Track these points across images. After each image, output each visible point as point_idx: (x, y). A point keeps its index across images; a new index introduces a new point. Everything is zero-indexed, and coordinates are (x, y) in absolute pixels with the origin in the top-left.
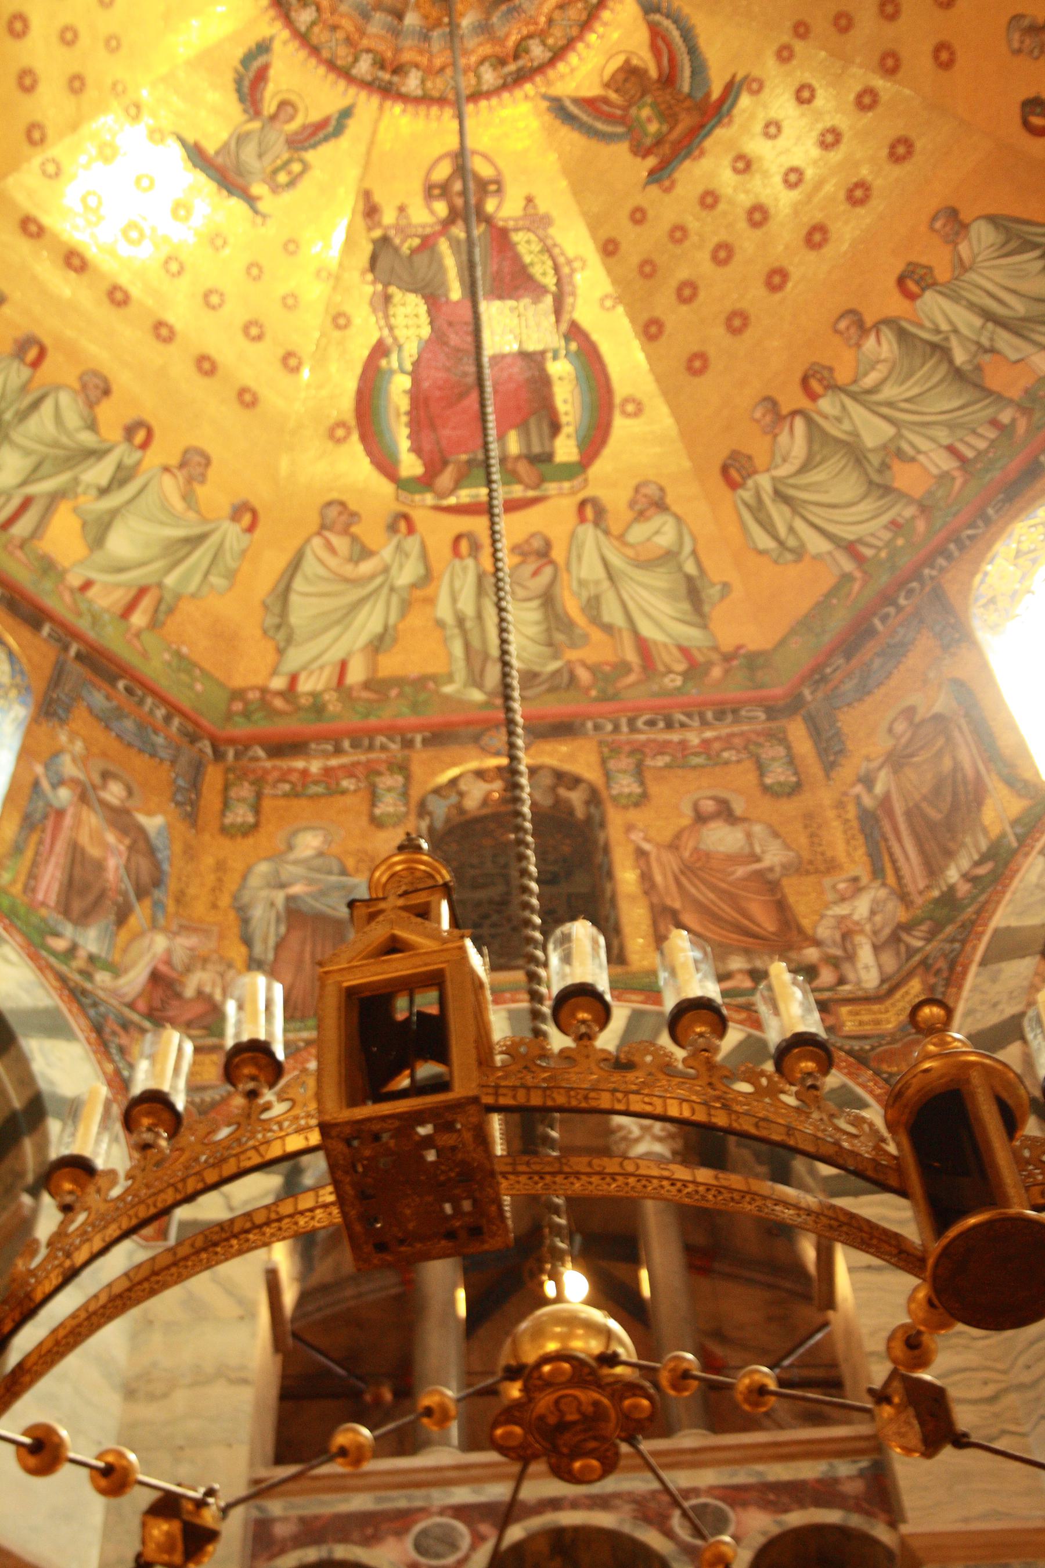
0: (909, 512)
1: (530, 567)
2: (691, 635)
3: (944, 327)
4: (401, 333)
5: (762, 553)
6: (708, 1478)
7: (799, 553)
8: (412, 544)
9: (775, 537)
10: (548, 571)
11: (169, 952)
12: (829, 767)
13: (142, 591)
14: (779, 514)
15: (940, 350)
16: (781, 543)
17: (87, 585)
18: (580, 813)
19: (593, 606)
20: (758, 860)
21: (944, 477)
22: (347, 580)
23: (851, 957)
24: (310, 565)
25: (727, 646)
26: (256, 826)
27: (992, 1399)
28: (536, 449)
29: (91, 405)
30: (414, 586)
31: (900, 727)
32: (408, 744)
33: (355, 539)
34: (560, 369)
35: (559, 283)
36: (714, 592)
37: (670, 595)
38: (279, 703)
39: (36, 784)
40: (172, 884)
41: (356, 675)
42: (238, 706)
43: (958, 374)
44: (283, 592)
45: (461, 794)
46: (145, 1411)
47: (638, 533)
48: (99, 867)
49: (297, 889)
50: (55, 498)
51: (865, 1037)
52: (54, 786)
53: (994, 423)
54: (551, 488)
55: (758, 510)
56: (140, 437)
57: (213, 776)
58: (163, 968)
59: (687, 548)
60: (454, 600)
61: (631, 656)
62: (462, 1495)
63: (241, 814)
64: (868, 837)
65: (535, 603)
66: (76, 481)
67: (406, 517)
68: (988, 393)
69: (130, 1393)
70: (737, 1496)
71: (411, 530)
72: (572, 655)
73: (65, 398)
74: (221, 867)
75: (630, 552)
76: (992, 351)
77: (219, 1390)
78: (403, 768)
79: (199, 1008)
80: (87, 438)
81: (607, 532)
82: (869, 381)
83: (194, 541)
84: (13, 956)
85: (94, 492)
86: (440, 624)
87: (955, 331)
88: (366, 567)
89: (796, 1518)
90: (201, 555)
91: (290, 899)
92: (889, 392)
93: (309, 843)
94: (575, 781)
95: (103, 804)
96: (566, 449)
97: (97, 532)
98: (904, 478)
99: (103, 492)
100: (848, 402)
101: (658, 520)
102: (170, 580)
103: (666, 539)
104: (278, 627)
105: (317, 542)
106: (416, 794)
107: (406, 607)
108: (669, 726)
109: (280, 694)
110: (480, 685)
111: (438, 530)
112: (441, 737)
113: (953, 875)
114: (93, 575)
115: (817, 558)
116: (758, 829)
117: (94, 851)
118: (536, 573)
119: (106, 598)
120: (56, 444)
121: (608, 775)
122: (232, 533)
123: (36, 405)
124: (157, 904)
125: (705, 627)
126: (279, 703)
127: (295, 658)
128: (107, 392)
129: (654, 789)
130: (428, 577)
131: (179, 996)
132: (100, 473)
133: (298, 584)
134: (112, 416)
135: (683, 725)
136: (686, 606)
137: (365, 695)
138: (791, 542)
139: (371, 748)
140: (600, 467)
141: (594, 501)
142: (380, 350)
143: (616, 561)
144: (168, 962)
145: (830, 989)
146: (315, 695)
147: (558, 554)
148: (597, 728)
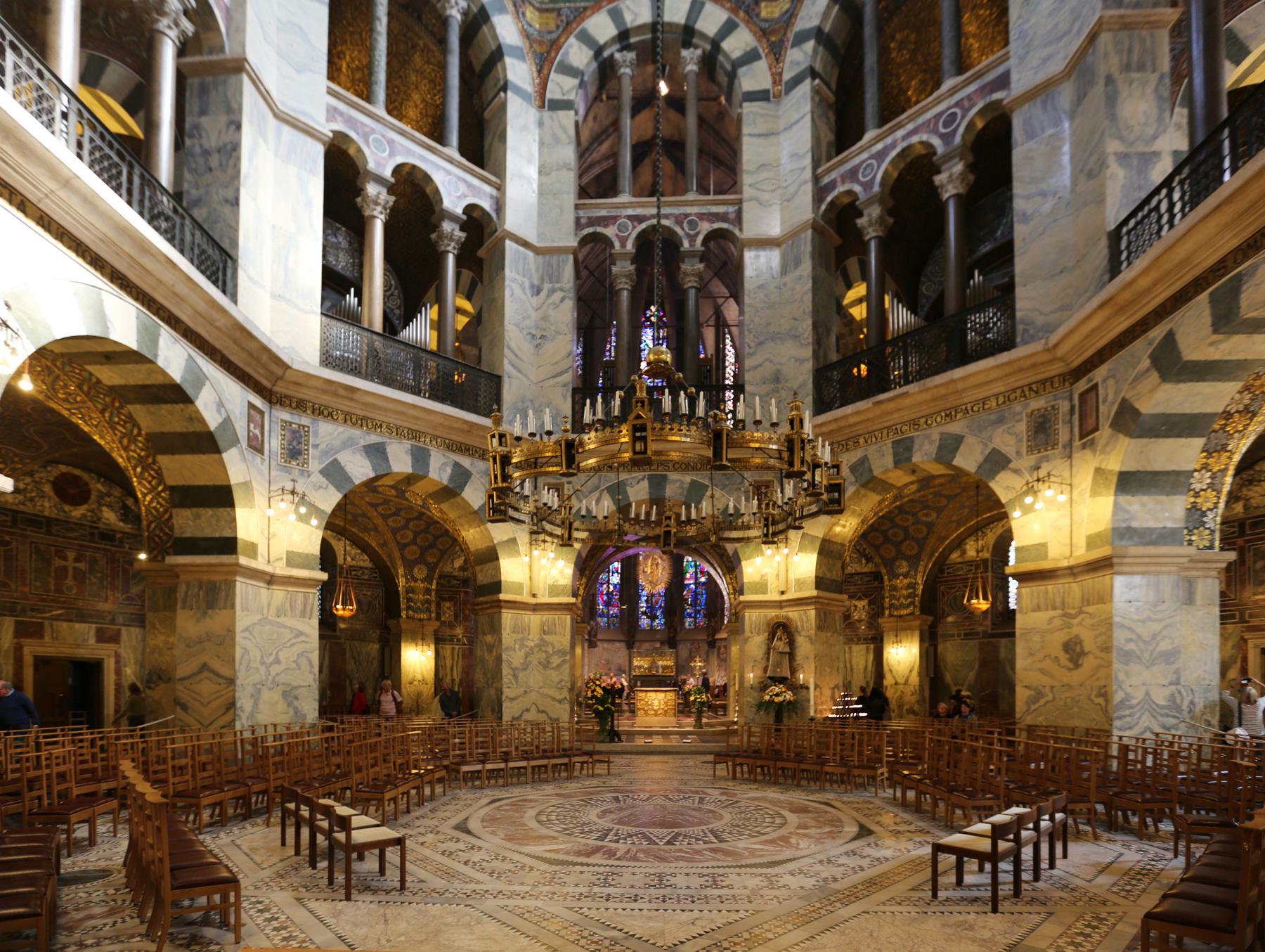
27: (773, 191)
51: (766, 20)
69: (540, 173)
70: (701, 216)
77: (564, 172)
89: (716, 225)
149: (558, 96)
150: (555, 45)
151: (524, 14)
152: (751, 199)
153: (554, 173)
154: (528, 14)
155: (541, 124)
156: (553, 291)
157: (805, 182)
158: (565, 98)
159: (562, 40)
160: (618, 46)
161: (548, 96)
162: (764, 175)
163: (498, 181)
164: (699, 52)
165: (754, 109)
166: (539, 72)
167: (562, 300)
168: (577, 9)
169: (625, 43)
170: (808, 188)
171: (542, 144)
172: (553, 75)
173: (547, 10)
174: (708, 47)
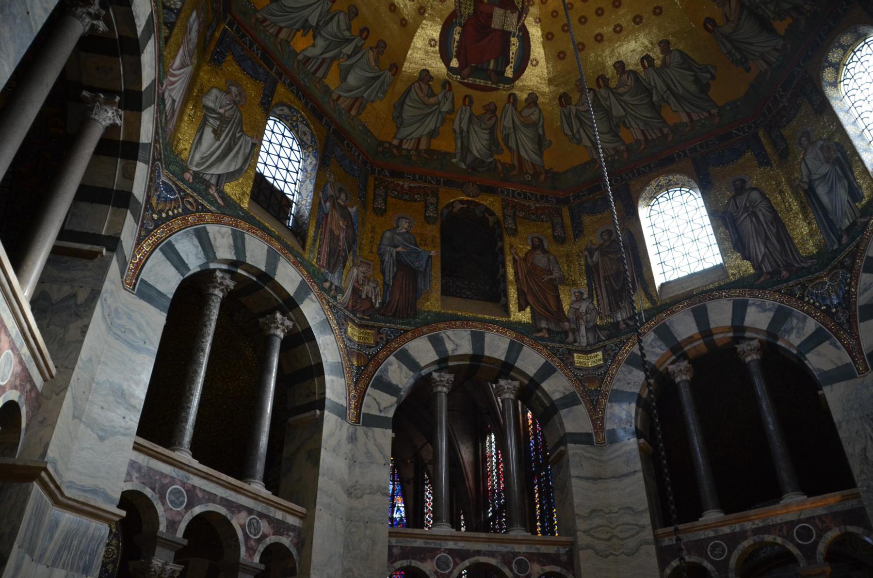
0: (622, 148)
1: (488, 116)
2: (536, 157)
3: (652, 84)
4: (463, 10)
5: (567, 135)
6: (523, 549)
7: (579, 142)
8: (449, 95)
9: (572, 131)
10: (494, 119)
11: (357, 275)
12: (576, 236)
13: (356, 99)
14: (575, 124)
15: (648, 92)
16: (574, 135)
17: (339, 97)
18: (491, 224)
19: (506, 138)
20: (552, 274)
21: (638, 141)
22: (424, 104)
23: (578, 330)
24: (413, 94)
25: (547, 168)
26: (385, 211)
28: (499, 69)
29: (350, 20)
30: (447, 112)
31: (606, 237)
32: (438, 182)
33: (430, 87)
34: (514, 40)
35: (522, 8)
38: (395, 151)
39: (320, 203)
40: (358, 242)
41: (423, 146)
42: (380, 149)
43: (652, 104)
44: (401, 103)
45: (453, 207)
46: (356, 503)
47: (526, 113)
48: (339, 240)
49: (399, 249)
50: (333, 59)
51: (579, 369)
52: (325, 203)
53: (661, 131)
54: (501, 86)
55: (568, 118)
56: (365, 34)
57: (371, 181)
58: (356, 285)
59: (541, 124)
60: (460, 123)
61: (516, 163)
62: (451, 545)
63: (380, 204)
64: (588, 278)
65: (487, 132)
66: (341, 52)
67: (449, 83)
68: (662, 118)
71: (450, 89)
72: (497, 157)
73: (342, 16)
74: (373, 230)
76: (667, 102)
77: (379, 497)
78: (436, 195)
80: (347, 33)
81: (516, 109)
82: (621, 90)
83: (375, 78)
84: (314, 298)
85: (346, 57)
86: (454, 131)
87: (656, 88)
88: (432, 100)
90: (377, 84)
91: (397, 253)
92: (626, 98)
93: (404, 225)
94: (492, 214)
95: (339, 204)
96: (509, 73)
97: (344, 74)
98: (623, 133)
99: (349, 57)
100: (611, 94)
101: (533, 109)
102: (365, 95)
103: (534, 117)
104: (398, 117)
105: (416, 84)
106: (440, 208)
107: (444, 121)
108: (525, 198)
109: (395, 146)
110: (465, 163)
111: (460, 91)
112: (449, 183)
113: (620, 317)
114: (341, 93)
115: (586, 147)
116: (551, 257)
117: (336, 232)
118: (489, 119)
119: (344, 104)
120: (336, 36)
121: (505, 219)
122: (388, 74)
123: (331, 19)
124: (355, 252)
125: (541, 156)
126: (395, 151)
127: (404, 132)
128: (357, 15)
129: (519, 228)
130: (452, 111)
131: (360, 296)
132: (348, 49)
133: (408, 101)
134: (356, 24)
135: (530, 199)
137: (425, 155)
138: (577, 136)
139: (425, 181)
140: (519, 83)
141: (514, 95)
142: (453, 15)
144: (357, 282)
146: (408, 151)
147: (498, 114)
148: (502, 192)
149: (374, 412)
153: (366, 497)
154: (349, 330)
155: (353, 439)
157: (647, 543)
158: (382, 414)
159: (381, 356)
160: (436, 367)
162: (598, 521)
163: (303, 510)
164: (516, 384)
165: (579, 451)
166: (356, 383)
169: (443, 365)
170: (652, 549)
171: (353, 461)
172: (370, 390)
173: (366, 327)
174: (526, 382)
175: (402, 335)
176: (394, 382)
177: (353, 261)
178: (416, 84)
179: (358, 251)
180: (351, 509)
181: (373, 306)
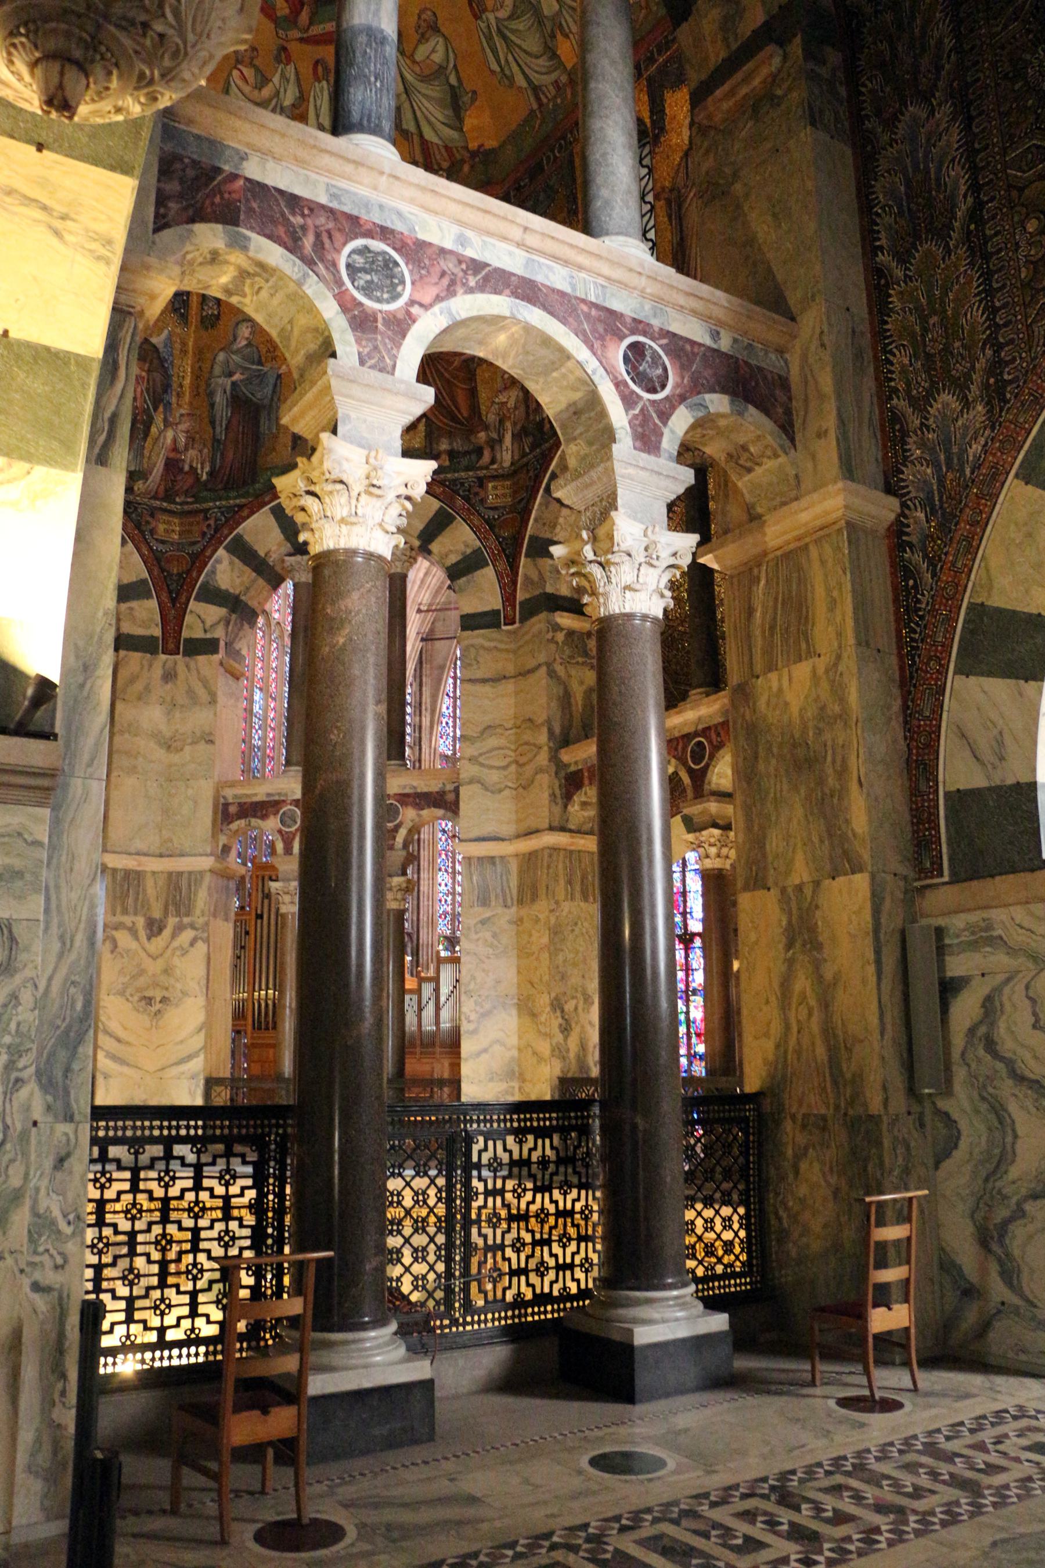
5: (493, 72)
7: (511, 79)
8: (290, 70)
11: (175, 440)
23: (501, 441)
25: (473, 145)
36: (466, 99)
37: (440, 103)
49: (237, 377)
58: (172, 455)
60: (318, 116)
67: (285, 49)
75: (417, 69)
79: (190, 480)
88: (266, 92)
91: (234, 384)
101: (432, 43)
103: (438, 57)
105: (235, 73)
131: (181, 470)
136: (450, 112)
143: (409, 77)
144: (175, 449)
145: (487, 468)
149: (199, 634)
150: (199, 560)
151: (152, 532)
152: (471, 782)
153: (187, 748)
154: (161, 527)
156: (179, 929)
158: (208, 636)
161: (185, 634)
167: (192, 944)
168: (229, 508)
172: (193, 605)
175: (236, 515)
176: (223, 587)
177: (165, 420)
178: (235, 73)
179: (174, 400)
180: (170, 766)
181: (198, 479)
